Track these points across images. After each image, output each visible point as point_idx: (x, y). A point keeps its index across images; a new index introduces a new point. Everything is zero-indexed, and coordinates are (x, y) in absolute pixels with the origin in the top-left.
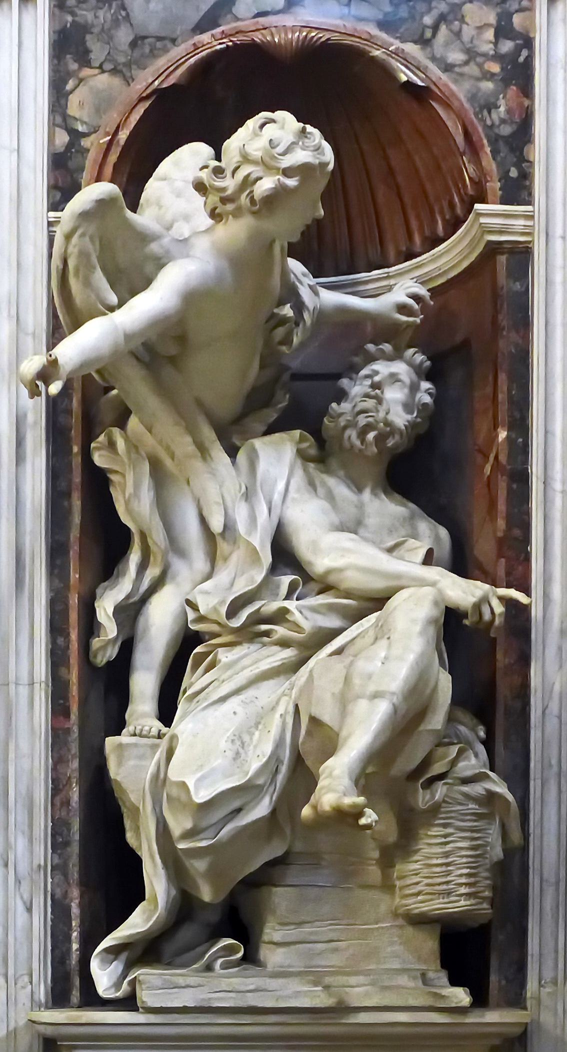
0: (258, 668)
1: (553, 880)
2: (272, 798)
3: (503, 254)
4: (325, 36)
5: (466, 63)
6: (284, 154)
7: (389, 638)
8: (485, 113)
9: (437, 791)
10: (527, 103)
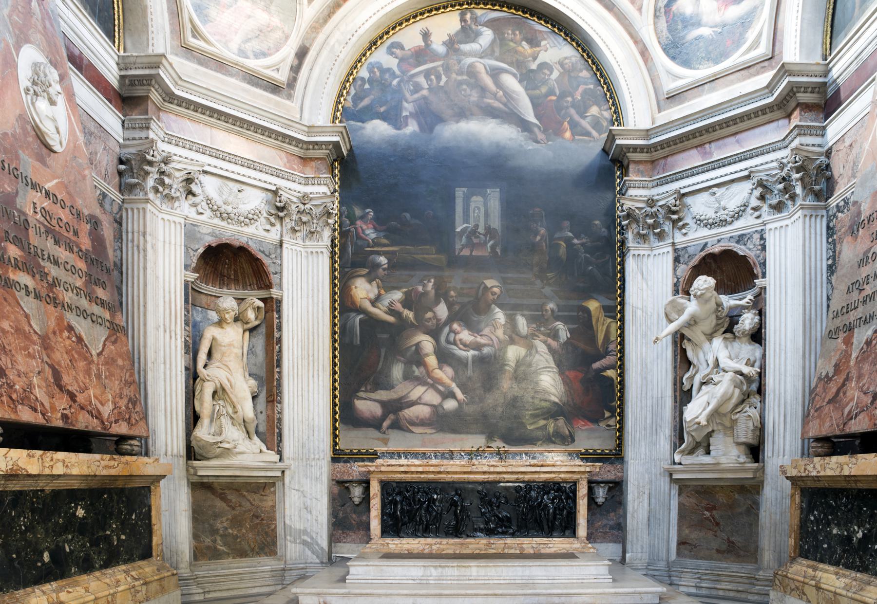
4: (724, 248)
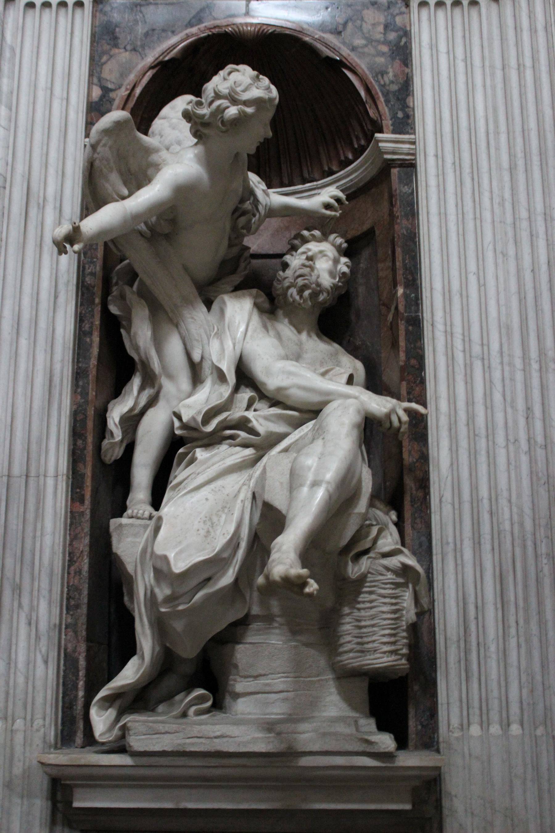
0: (224, 463)
1: (455, 639)
2: (234, 569)
3: (395, 167)
5: (366, 46)
6: (244, 91)
7: (323, 439)
8: (380, 77)
9: (363, 564)
10: (407, 70)
